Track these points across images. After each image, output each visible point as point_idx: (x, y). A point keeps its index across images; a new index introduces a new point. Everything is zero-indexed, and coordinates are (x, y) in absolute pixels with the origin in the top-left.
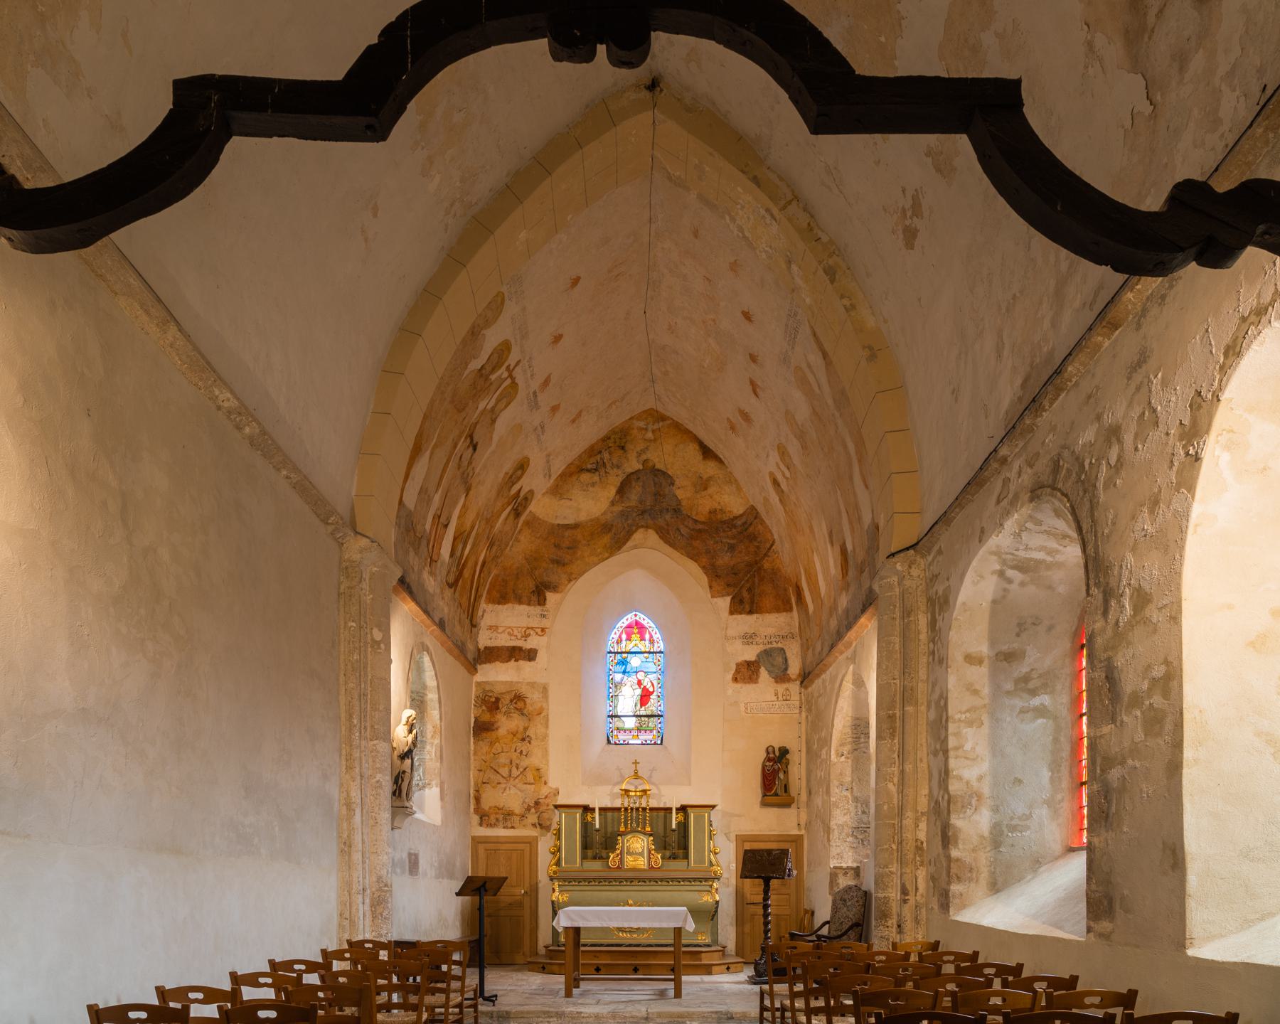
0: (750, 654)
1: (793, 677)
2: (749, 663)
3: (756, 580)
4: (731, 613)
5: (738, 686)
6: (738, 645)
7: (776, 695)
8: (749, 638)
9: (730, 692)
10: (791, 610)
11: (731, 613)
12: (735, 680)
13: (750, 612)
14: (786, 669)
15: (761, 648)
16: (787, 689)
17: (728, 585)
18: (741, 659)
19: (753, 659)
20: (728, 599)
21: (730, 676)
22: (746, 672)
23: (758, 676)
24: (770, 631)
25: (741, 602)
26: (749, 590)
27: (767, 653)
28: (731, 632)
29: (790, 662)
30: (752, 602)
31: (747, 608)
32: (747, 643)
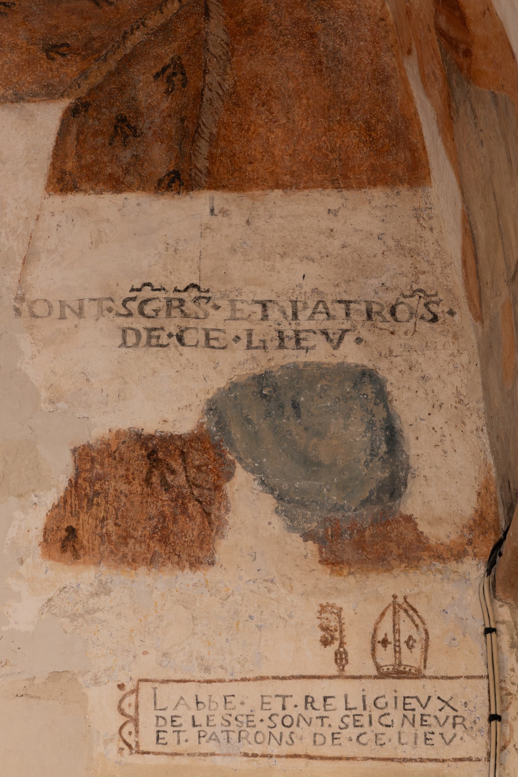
0: (168, 396)
1: (439, 534)
2: (155, 452)
3: (216, 30)
4: (63, 180)
5: (83, 576)
6: (95, 347)
7: (331, 636)
8: (158, 315)
9: (25, 613)
10: (415, 173)
11: (63, 180)
12: (65, 541)
13: (177, 181)
14: (394, 488)
15: (234, 365)
16: (402, 607)
17: (54, 49)
18: (104, 423)
19: (185, 424)
20: (49, 116)
21: (32, 520)
22: (143, 500)
23: (211, 523)
24: (291, 278)
25: (125, 128)
26: (173, 75)
27: (269, 405)
28: (48, 280)
29: (419, 448)
30: (188, 132)
31: (160, 158)
32: (152, 339)
